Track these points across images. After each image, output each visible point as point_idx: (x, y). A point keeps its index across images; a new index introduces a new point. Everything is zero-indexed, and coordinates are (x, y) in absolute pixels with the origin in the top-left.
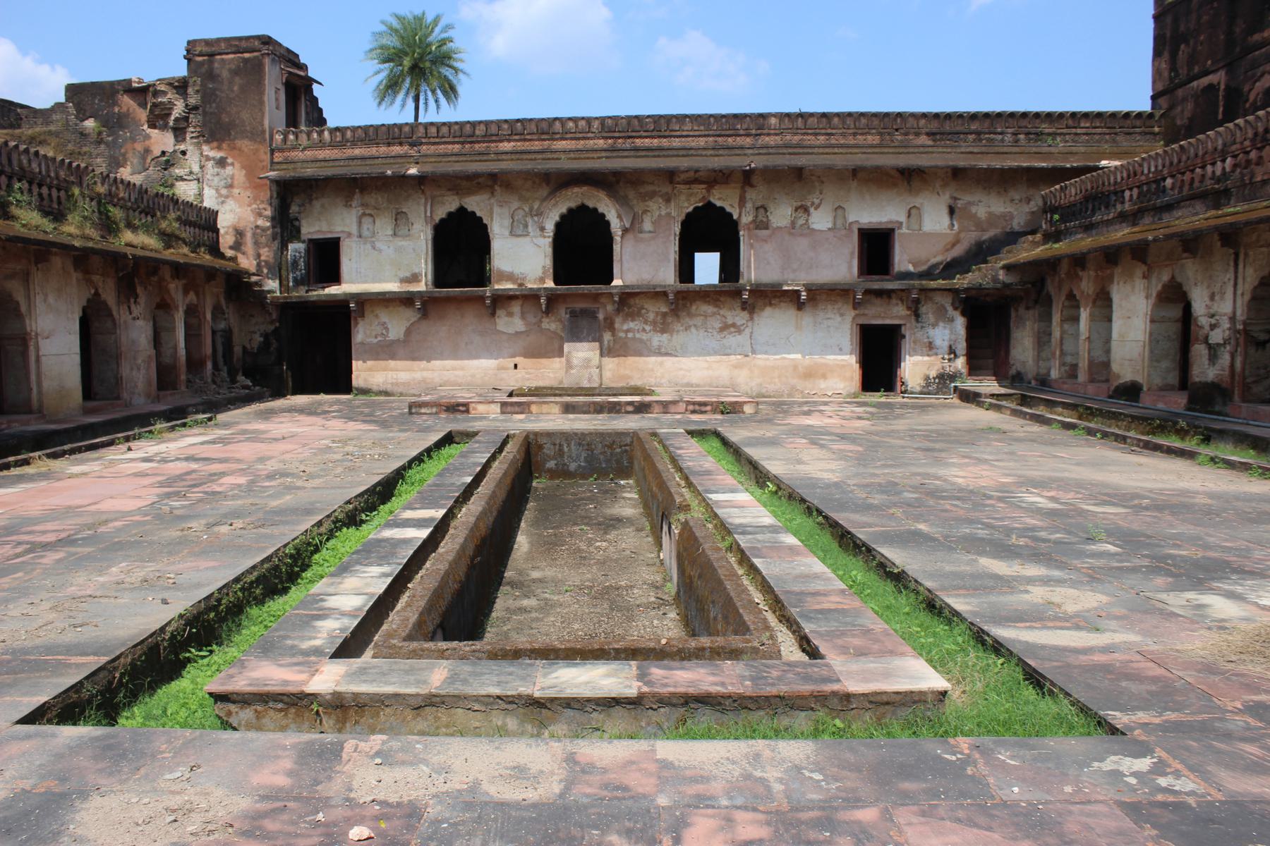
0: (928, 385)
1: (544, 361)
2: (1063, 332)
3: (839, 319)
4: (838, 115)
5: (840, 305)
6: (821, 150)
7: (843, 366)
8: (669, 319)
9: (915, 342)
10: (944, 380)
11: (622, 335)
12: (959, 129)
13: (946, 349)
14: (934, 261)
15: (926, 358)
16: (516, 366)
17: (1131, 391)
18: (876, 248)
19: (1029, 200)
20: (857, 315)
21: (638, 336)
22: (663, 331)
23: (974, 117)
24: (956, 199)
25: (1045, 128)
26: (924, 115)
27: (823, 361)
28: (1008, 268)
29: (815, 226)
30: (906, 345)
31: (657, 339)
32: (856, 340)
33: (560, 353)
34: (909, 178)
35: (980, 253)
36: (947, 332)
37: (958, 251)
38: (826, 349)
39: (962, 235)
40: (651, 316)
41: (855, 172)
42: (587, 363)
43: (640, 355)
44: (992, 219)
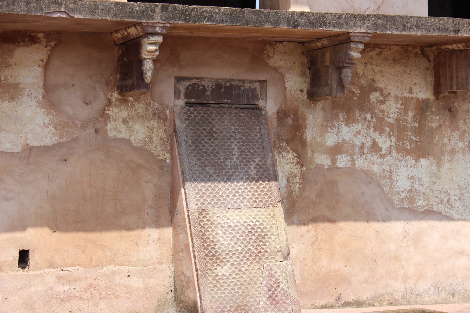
1: (112, 238)
8: (434, 121)
11: (323, 160)
16: (24, 257)
21: (360, 163)
22: (420, 152)
31: (407, 173)
33: (167, 210)
40: (392, 109)
42: (256, 245)
43: (369, 217)
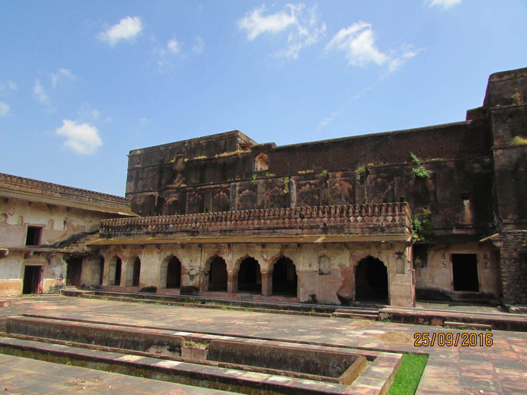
0: (51, 290)
2: (109, 270)
3: (17, 263)
4: (26, 179)
5: (18, 257)
6: (17, 192)
7: (17, 283)
9: (47, 273)
10: (58, 287)
12: (70, 193)
13: (59, 275)
14: (57, 241)
15: (51, 279)
17: (153, 289)
18: (33, 234)
19: (91, 222)
20: (25, 262)
23: (77, 190)
24: (67, 218)
25: (99, 198)
26: (59, 186)
27: (7, 281)
28: (88, 246)
29: (10, 223)
30: (44, 274)
32: (23, 272)
34: (51, 208)
35: (74, 240)
36: (60, 269)
37: (66, 238)
38: (10, 276)
39: (68, 232)
41: (30, 203)
44: (79, 227)
